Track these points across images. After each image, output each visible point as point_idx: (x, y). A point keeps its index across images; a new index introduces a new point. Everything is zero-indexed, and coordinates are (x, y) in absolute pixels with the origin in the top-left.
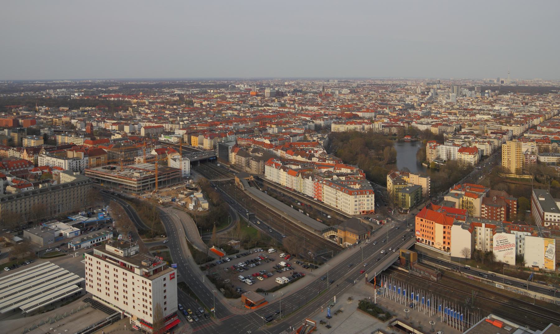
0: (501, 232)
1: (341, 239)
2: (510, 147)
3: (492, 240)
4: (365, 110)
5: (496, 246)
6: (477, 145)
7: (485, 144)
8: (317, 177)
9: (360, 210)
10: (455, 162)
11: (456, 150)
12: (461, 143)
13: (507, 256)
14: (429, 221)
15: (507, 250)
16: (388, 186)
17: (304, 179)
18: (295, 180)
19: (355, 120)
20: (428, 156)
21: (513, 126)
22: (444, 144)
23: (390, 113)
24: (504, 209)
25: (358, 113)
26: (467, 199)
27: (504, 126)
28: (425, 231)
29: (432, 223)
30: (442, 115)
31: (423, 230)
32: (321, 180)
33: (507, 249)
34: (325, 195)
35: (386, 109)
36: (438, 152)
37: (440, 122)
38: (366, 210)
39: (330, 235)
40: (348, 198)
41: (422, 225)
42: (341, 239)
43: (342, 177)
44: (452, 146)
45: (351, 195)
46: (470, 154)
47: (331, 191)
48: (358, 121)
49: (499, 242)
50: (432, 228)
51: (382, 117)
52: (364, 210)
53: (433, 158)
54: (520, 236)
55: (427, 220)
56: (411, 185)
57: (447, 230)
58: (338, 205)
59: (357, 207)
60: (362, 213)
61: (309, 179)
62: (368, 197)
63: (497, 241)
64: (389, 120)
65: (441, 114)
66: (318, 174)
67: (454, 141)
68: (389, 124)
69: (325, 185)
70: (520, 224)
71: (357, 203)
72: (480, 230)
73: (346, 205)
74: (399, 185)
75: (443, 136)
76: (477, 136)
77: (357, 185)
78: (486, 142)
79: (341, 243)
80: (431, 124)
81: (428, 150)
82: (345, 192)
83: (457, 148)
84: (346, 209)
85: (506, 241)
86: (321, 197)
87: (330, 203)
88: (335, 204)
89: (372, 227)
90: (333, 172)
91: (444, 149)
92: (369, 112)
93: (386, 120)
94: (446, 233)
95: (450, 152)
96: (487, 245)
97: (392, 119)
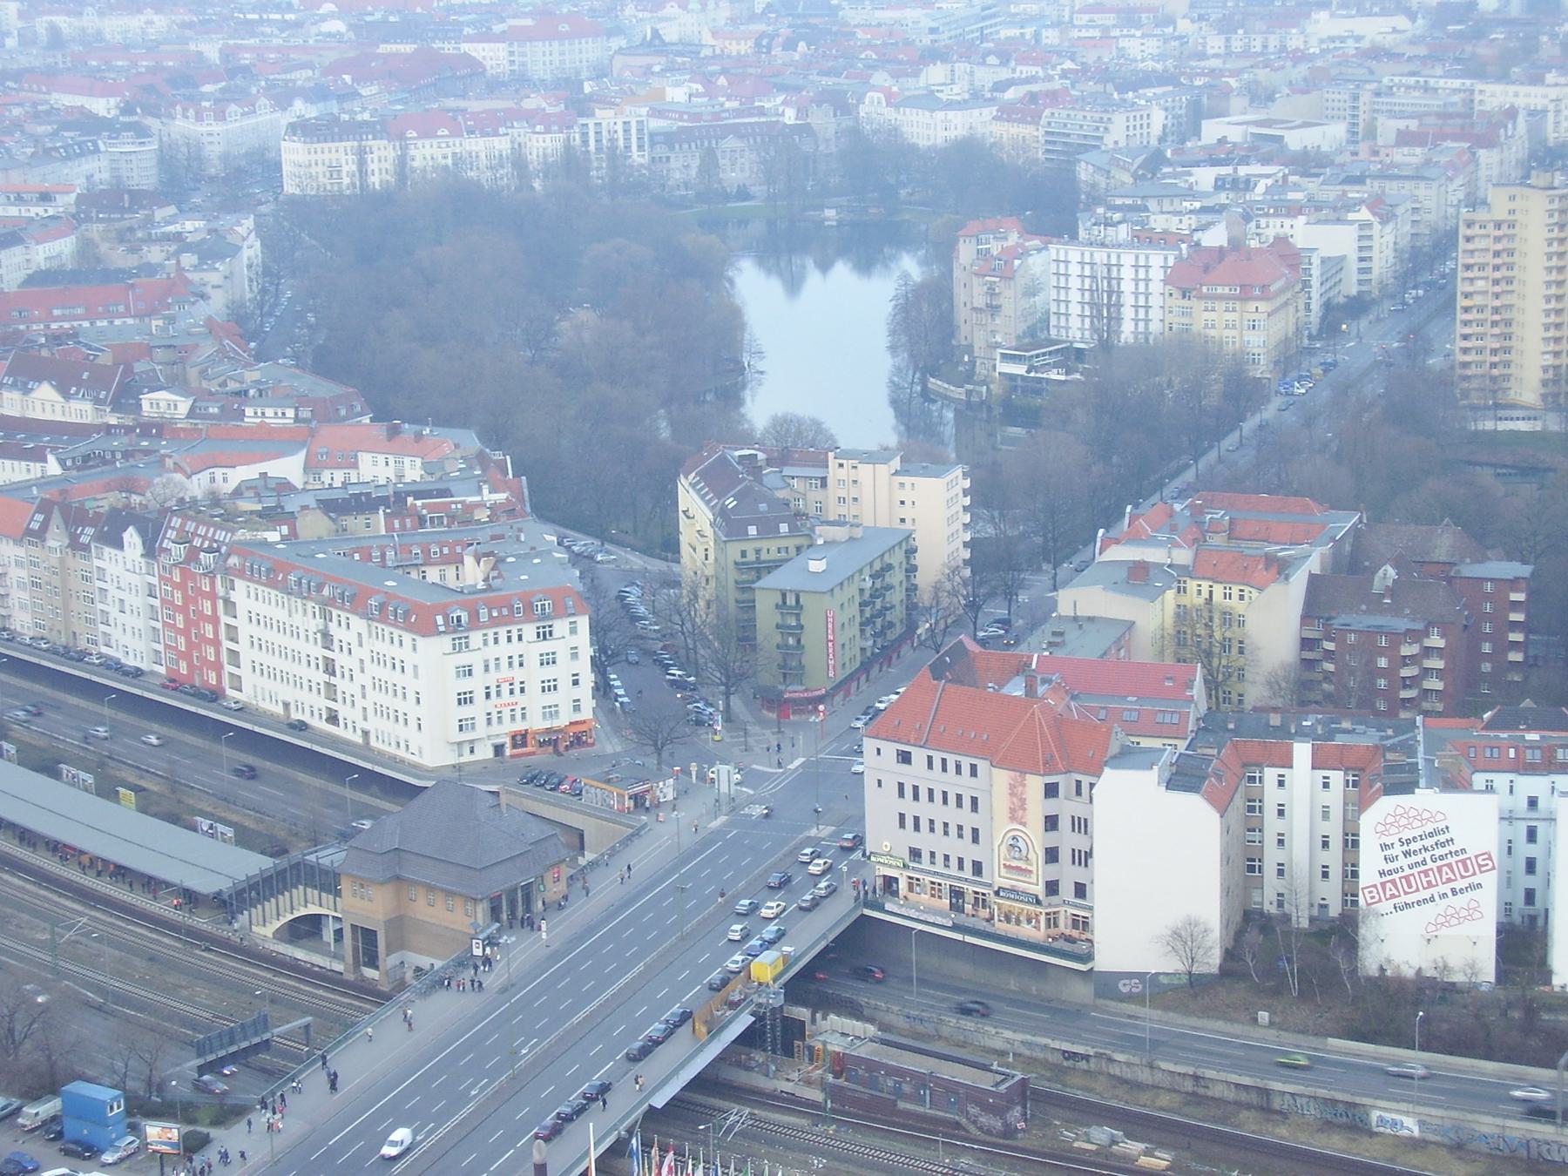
0: (1408, 787)
1: (368, 936)
2: (1512, 225)
3: (1355, 844)
4: (529, 22)
5: (1378, 880)
6: (1301, 232)
7: (1351, 216)
8: (181, 530)
9: (496, 729)
10: (1149, 357)
11: (1157, 274)
12: (1189, 222)
13: (1444, 931)
14: (951, 760)
15: (1445, 895)
16: (685, 549)
17: (86, 548)
18: (19, 564)
19: (451, 103)
20: (973, 332)
21: (1551, 77)
22: (1074, 236)
23: (707, 39)
24: (1441, 643)
25: (478, 51)
26: (1205, 594)
27: (1490, 88)
28: (924, 825)
29: (974, 769)
30: (1075, 34)
31: (916, 819)
32: (210, 550)
33: (1446, 889)
34: (242, 647)
35: (684, 6)
36: (1031, 291)
37: (1057, 84)
38: (537, 723)
39: (290, 917)
40: (405, 653)
41: (909, 792)
42: (368, 936)
43: (361, 519)
44: (1129, 245)
45: (428, 630)
46: (1245, 295)
47: (279, 614)
48: (474, 106)
49: (1397, 850)
50: (974, 801)
51: (649, 67)
52: (520, 726)
53: (999, 339)
54: (1533, 803)
55: (937, 757)
56: (839, 533)
57: (1066, 808)
58: (343, 711)
59: (478, 710)
60: (508, 752)
61: (119, 544)
62: (544, 636)
63: (1384, 847)
64: (700, 88)
65: (1071, 21)
66: (187, 508)
67: (1146, 209)
68: (696, 117)
69: (240, 584)
70: (1529, 729)
71: (476, 684)
72: (1281, 784)
73: (398, 703)
74: (762, 534)
75: (1073, 179)
76: (1308, 163)
77: (469, 560)
78: (1362, 201)
79: (373, 962)
80: (992, 100)
81: (969, 293)
82: (383, 620)
83: (1158, 261)
84: (400, 731)
85: (1442, 838)
86: (217, 667)
87: (286, 705)
88: (322, 703)
89: (581, 836)
90: (298, 482)
91: (1074, 270)
92: (561, 37)
93: (677, 94)
94: (1064, 824)
95: (1114, 292)
96: (1325, 875)
97: (722, 81)
